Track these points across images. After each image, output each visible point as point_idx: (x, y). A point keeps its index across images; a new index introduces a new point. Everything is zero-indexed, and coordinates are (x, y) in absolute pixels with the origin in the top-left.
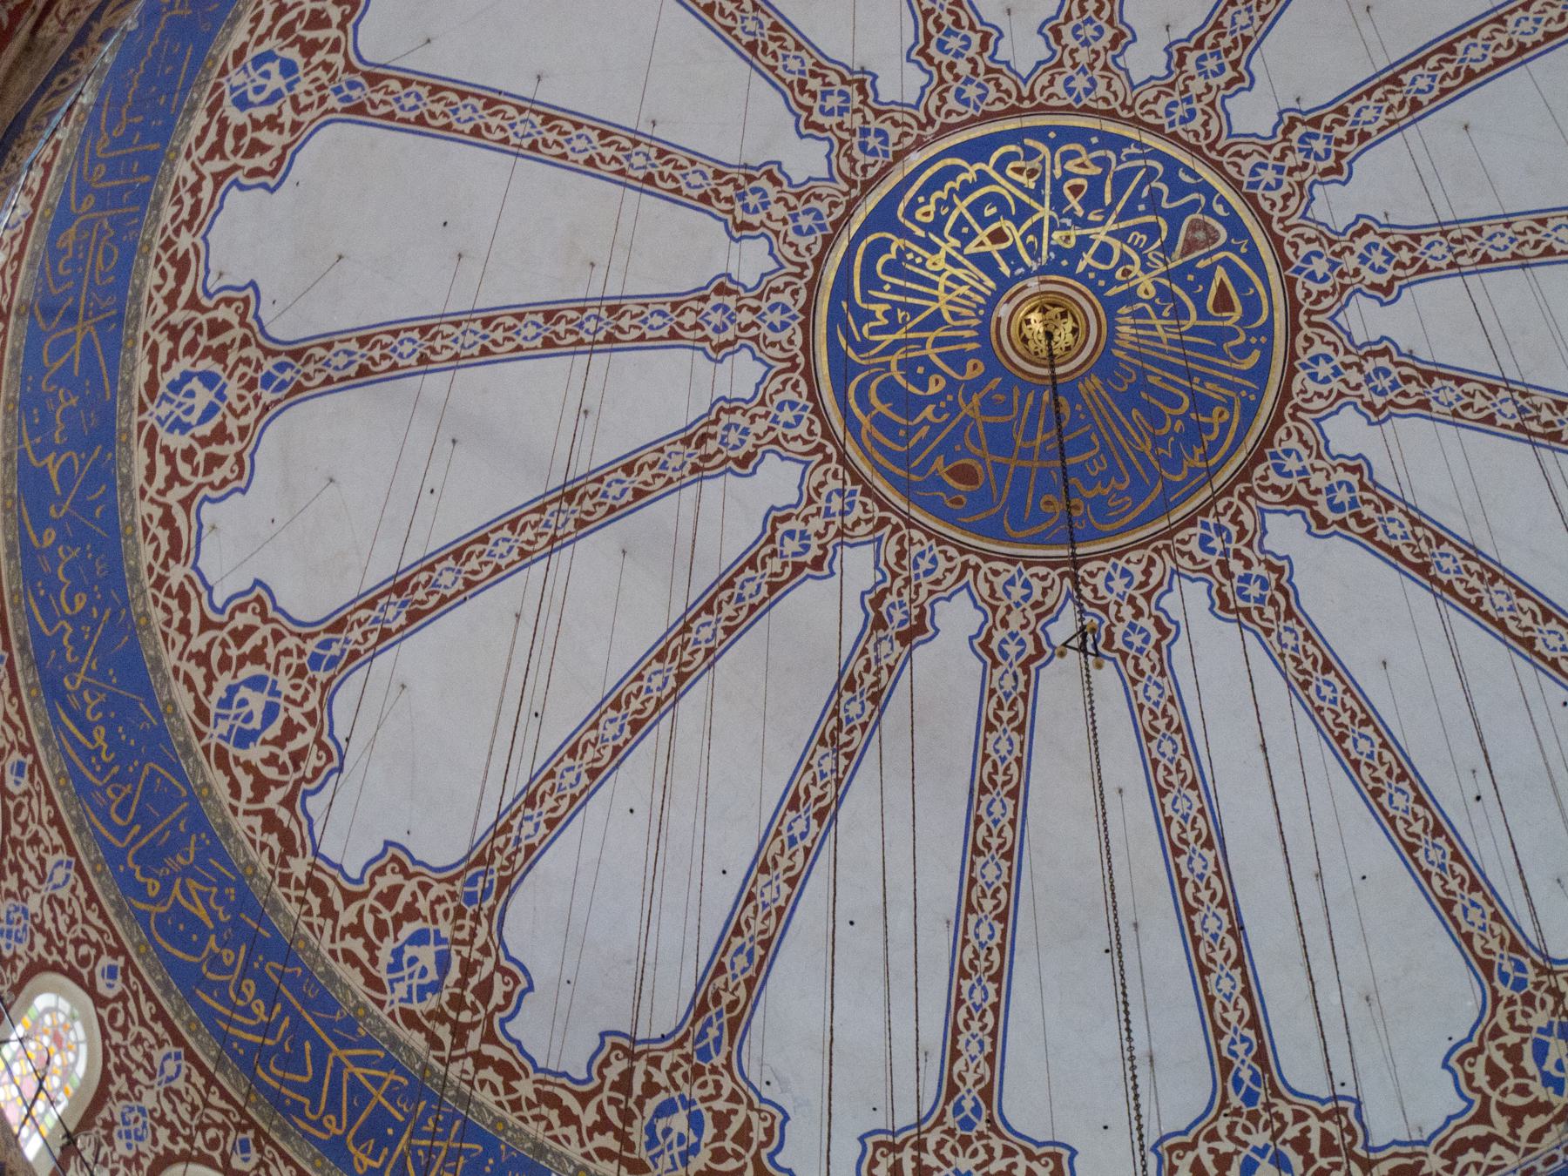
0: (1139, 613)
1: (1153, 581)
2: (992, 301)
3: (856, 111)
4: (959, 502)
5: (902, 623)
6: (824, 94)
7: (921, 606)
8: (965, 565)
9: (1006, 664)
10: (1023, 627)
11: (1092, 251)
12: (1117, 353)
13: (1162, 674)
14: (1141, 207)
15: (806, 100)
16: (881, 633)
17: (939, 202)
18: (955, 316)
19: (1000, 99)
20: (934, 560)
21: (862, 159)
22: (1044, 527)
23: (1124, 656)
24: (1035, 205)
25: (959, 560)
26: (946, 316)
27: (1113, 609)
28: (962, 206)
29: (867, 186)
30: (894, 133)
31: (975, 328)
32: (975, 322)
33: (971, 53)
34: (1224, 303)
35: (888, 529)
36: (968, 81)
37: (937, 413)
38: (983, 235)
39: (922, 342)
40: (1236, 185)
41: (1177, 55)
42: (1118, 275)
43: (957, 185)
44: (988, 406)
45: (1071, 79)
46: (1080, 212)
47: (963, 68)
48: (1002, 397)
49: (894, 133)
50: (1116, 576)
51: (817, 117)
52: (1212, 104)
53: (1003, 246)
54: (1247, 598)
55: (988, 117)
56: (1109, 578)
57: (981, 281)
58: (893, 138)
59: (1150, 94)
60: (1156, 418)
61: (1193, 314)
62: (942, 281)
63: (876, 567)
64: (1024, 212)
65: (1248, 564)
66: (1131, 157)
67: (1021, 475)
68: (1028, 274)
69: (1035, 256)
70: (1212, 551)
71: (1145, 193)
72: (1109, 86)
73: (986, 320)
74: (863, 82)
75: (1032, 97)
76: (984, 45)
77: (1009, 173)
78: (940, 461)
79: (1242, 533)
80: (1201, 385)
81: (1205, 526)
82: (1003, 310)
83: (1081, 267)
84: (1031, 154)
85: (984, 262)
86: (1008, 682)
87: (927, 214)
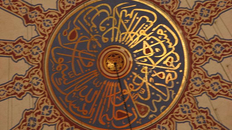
0: (26, 87)
1: (35, 92)
2: (126, 47)
3: (200, 18)
4: (65, 34)
5: (30, 16)
6: (209, 11)
7: (34, 22)
8: (45, 35)
9: (13, 47)
10: (24, 52)
11: (139, 77)
12: (105, 82)
13: (7, 95)
14: (153, 94)
15: (208, 5)
16: (29, 10)
17: (163, 36)
18: (123, 36)
19: (196, 59)
20: (48, 26)
21: (183, 18)
22: (54, 59)
23: (13, 83)
24: (158, 63)
25: (47, 33)
26: (123, 33)
27: (27, 79)
28: (161, 43)
29: (173, 18)
30: (190, 27)
31: (118, 41)
32: (120, 41)
33: (213, 53)
34: (120, 115)
35: (60, 12)
36: (204, 51)
37: (93, 29)
38: (150, 47)
39: (117, 26)
40: (159, 122)
41: (205, 111)
42: (131, 84)
43: (168, 42)
44: (93, 43)
45: (200, 80)
46: (153, 75)
47: (209, 50)
48: (94, 47)
49: (190, 27)
50: (37, 81)
51: (201, 7)
52: (187, 118)
53: (144, 52)
54: (29, 121)
55: (190, 54)
56: (37, 78)
57: (133, 44)
58: (188, 27)
59: (192, 101)
60: (84, 93)
61: (116, 106)
62: (136, 33)
63: (49, 9)
64: (156, 60)
65: (39, 121)
66: (171, 93)
67: (70, 52)
68: (134, 58)
69: (139, 61)
70: (43, 110)
71: (158, 95)
72: (197, 90)
73: (120, 44)
74: (210, 21)
75: (195, 68)
76: (215, 57)
77: (170, 57)
78: (79, 29)
79: (49, 119)
80: (94, 107)
81: (51, 108)
82: (123, 49)
83: (134, 74)
84: (175, 64)
85: (140, 46)
86: (8, 48)
87: (160, 32)
